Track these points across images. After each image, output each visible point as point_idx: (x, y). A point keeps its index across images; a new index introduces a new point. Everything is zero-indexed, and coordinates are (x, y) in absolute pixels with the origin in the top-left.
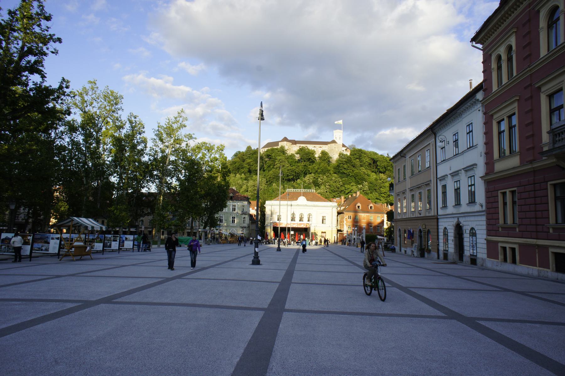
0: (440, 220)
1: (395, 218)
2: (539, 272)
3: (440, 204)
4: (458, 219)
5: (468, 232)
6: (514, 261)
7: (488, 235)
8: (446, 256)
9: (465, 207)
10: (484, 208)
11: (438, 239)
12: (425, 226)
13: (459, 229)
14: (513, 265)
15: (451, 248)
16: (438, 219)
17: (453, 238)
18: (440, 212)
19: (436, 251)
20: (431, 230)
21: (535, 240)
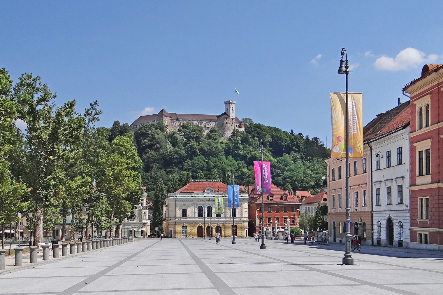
0: (374, 215)
1: (329, 212)
2: (439, 247)
3: (375, 203)
4: (389, 215)
5: (397, 224)
6: (426, 242)
7: (411, 226)
8: (379, 242)
9: (394, 206)
10: (409, 208)
11: (373, 230)
12: (361, 219)
13: (390, 222)
14: (426, 245)
15: (384, 237)
16: (372, 214)
17: (385, 229)
18: (375, 209)
19: (371, 238)
20: (366, 223)
21: (438, 229)
